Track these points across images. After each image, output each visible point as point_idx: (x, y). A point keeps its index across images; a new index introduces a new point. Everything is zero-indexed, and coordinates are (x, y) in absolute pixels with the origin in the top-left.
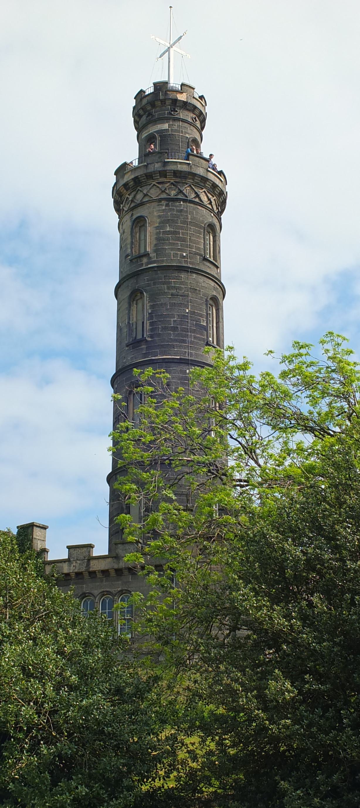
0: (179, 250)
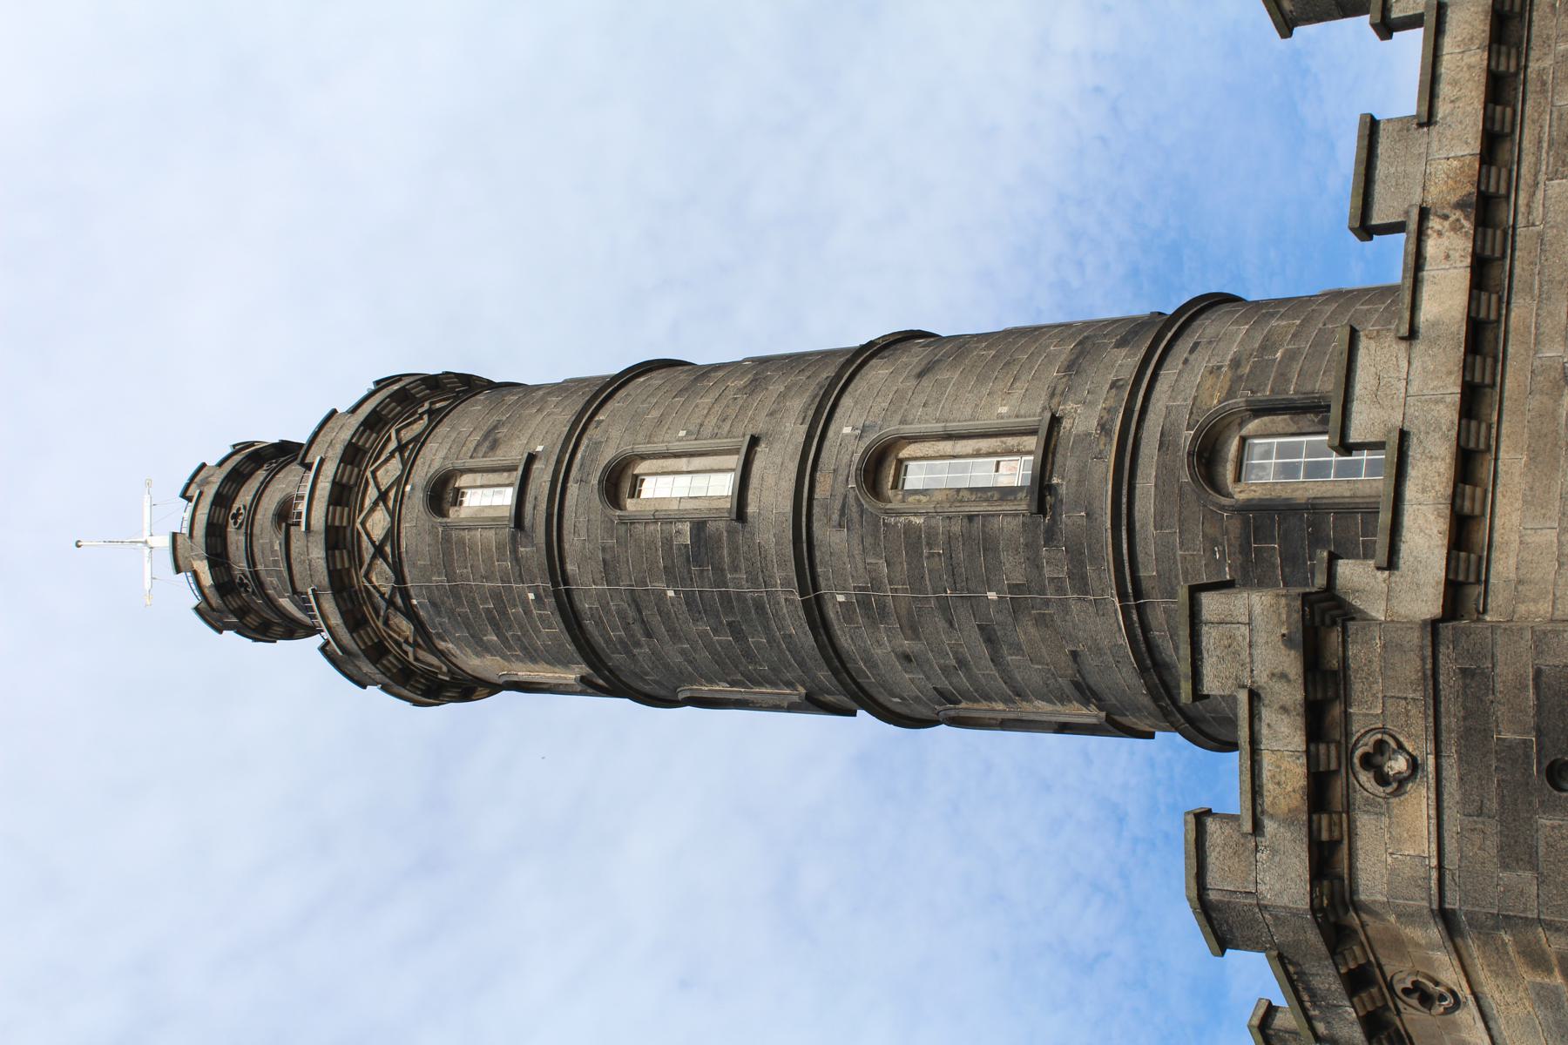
0: (527, 612)
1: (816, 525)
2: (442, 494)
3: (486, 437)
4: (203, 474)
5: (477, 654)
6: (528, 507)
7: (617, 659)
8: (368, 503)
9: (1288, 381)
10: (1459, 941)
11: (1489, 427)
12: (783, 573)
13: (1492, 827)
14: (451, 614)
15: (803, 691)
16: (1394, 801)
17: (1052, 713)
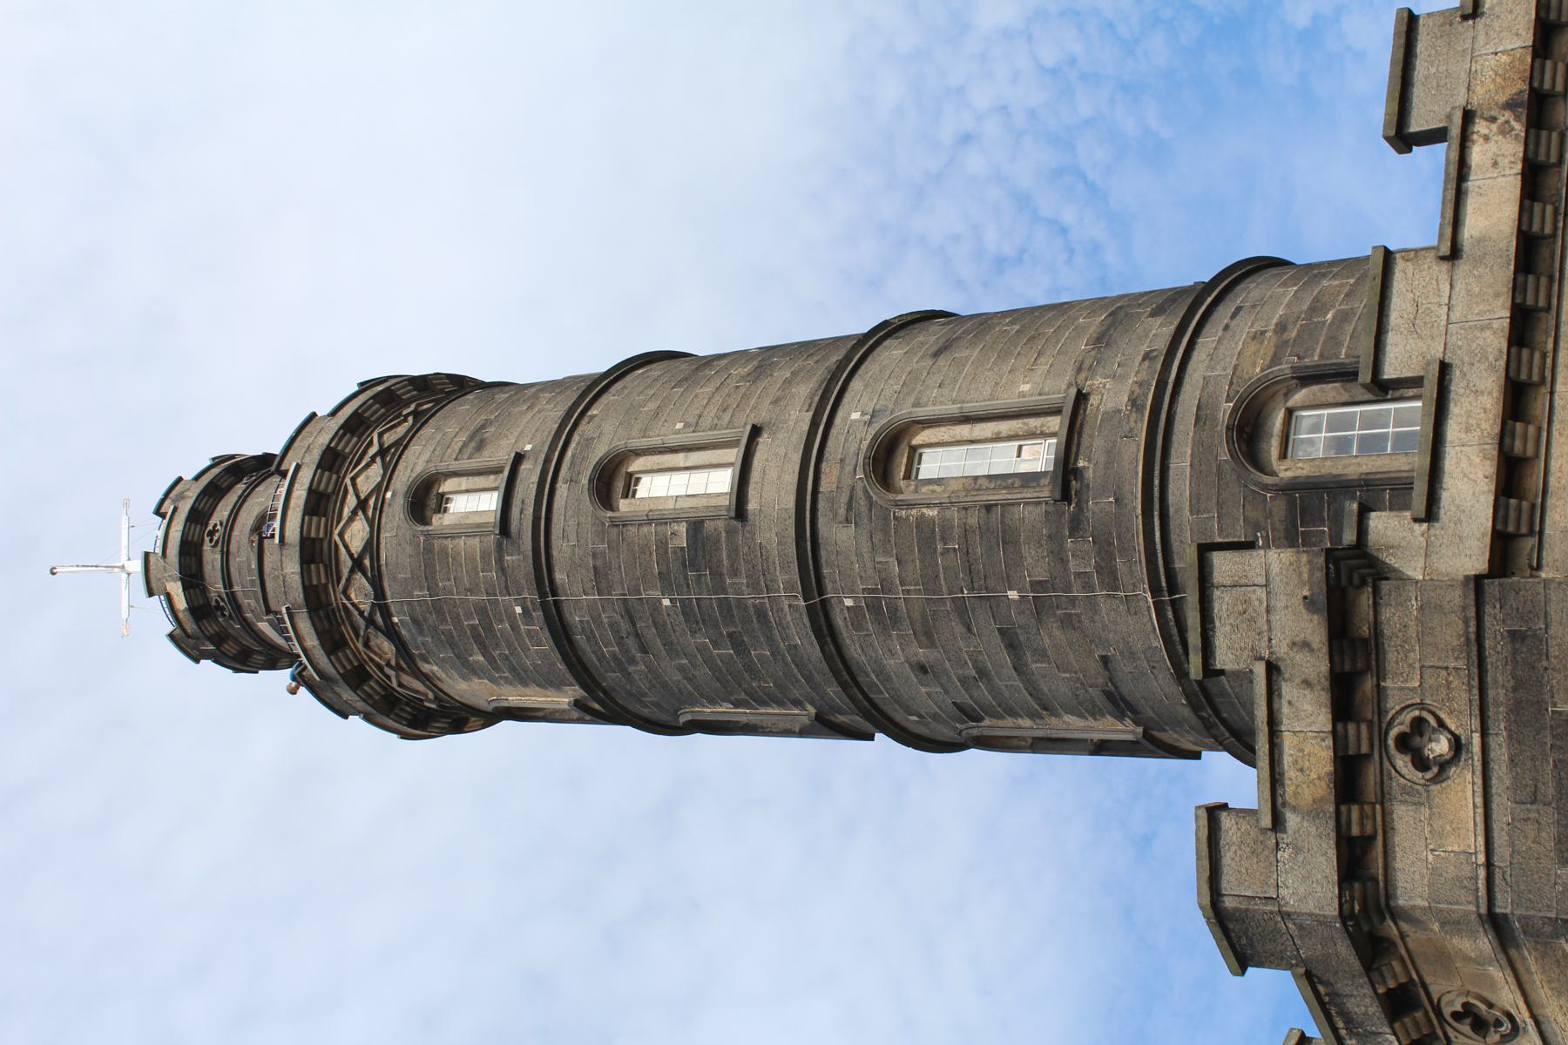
0: (514, 627)
1: (821, 521)
2: (424, 499)
3: (472, 437)
4: (178, 488)
5: (464, 678)
6: (515, 511)
7: (611, 678)
8: (346, 512)
9: (1340, 344)
10: (1513, 952)
11: (1544, 356)
12: (785, 576)
13: (1548, 816)
14: (434, 631)
15: (812, 710)
16: (1433, 787)
17: (1083, 730)
